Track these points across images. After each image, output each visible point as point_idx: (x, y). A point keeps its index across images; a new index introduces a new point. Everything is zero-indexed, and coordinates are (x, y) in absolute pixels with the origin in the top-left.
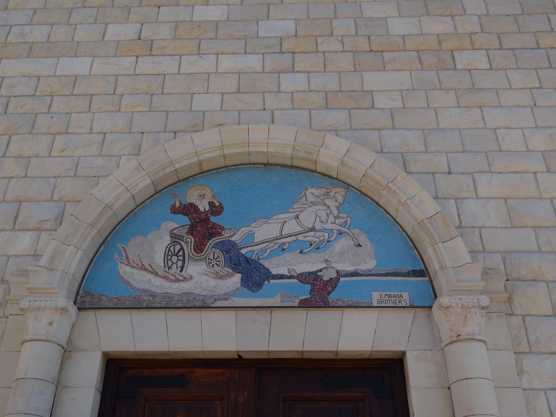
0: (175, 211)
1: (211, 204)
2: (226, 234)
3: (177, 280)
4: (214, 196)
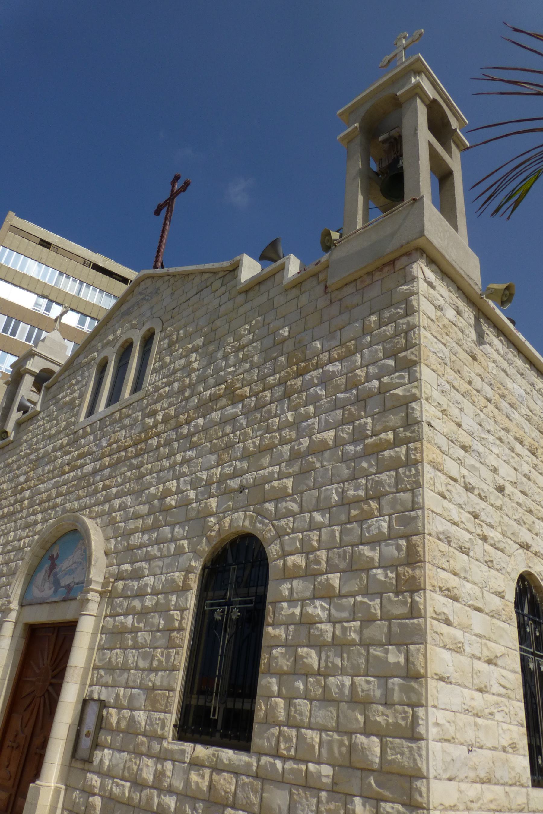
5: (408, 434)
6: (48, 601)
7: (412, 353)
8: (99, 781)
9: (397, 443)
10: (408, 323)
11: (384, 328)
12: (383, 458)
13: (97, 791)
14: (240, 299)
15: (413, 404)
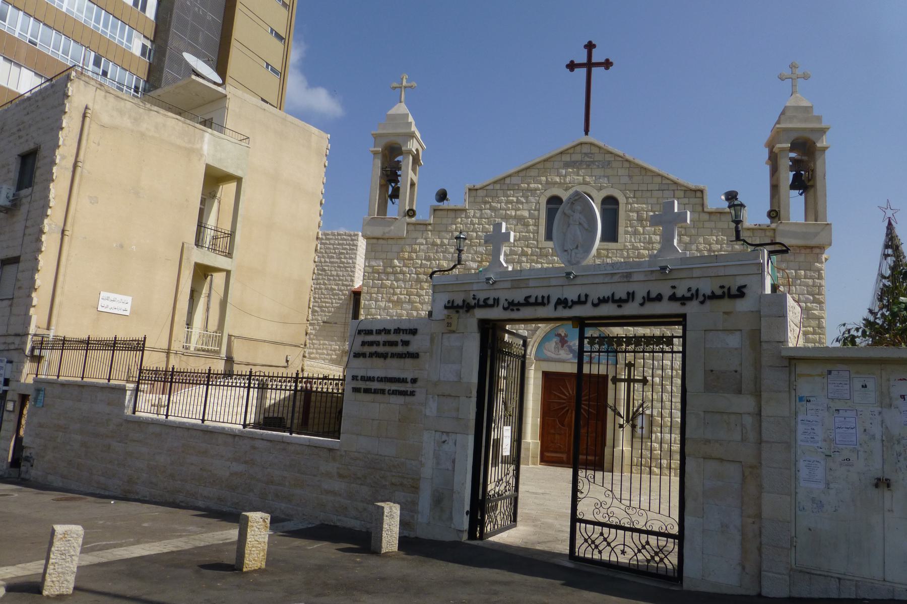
0: (556, 335)
1: (565, 334)
2: (569, 343)
3: (557, 355)
9: (814, 333)
10: (820, 283)
12: (809, 338)
13: (658, 449)
14: (706, 217)
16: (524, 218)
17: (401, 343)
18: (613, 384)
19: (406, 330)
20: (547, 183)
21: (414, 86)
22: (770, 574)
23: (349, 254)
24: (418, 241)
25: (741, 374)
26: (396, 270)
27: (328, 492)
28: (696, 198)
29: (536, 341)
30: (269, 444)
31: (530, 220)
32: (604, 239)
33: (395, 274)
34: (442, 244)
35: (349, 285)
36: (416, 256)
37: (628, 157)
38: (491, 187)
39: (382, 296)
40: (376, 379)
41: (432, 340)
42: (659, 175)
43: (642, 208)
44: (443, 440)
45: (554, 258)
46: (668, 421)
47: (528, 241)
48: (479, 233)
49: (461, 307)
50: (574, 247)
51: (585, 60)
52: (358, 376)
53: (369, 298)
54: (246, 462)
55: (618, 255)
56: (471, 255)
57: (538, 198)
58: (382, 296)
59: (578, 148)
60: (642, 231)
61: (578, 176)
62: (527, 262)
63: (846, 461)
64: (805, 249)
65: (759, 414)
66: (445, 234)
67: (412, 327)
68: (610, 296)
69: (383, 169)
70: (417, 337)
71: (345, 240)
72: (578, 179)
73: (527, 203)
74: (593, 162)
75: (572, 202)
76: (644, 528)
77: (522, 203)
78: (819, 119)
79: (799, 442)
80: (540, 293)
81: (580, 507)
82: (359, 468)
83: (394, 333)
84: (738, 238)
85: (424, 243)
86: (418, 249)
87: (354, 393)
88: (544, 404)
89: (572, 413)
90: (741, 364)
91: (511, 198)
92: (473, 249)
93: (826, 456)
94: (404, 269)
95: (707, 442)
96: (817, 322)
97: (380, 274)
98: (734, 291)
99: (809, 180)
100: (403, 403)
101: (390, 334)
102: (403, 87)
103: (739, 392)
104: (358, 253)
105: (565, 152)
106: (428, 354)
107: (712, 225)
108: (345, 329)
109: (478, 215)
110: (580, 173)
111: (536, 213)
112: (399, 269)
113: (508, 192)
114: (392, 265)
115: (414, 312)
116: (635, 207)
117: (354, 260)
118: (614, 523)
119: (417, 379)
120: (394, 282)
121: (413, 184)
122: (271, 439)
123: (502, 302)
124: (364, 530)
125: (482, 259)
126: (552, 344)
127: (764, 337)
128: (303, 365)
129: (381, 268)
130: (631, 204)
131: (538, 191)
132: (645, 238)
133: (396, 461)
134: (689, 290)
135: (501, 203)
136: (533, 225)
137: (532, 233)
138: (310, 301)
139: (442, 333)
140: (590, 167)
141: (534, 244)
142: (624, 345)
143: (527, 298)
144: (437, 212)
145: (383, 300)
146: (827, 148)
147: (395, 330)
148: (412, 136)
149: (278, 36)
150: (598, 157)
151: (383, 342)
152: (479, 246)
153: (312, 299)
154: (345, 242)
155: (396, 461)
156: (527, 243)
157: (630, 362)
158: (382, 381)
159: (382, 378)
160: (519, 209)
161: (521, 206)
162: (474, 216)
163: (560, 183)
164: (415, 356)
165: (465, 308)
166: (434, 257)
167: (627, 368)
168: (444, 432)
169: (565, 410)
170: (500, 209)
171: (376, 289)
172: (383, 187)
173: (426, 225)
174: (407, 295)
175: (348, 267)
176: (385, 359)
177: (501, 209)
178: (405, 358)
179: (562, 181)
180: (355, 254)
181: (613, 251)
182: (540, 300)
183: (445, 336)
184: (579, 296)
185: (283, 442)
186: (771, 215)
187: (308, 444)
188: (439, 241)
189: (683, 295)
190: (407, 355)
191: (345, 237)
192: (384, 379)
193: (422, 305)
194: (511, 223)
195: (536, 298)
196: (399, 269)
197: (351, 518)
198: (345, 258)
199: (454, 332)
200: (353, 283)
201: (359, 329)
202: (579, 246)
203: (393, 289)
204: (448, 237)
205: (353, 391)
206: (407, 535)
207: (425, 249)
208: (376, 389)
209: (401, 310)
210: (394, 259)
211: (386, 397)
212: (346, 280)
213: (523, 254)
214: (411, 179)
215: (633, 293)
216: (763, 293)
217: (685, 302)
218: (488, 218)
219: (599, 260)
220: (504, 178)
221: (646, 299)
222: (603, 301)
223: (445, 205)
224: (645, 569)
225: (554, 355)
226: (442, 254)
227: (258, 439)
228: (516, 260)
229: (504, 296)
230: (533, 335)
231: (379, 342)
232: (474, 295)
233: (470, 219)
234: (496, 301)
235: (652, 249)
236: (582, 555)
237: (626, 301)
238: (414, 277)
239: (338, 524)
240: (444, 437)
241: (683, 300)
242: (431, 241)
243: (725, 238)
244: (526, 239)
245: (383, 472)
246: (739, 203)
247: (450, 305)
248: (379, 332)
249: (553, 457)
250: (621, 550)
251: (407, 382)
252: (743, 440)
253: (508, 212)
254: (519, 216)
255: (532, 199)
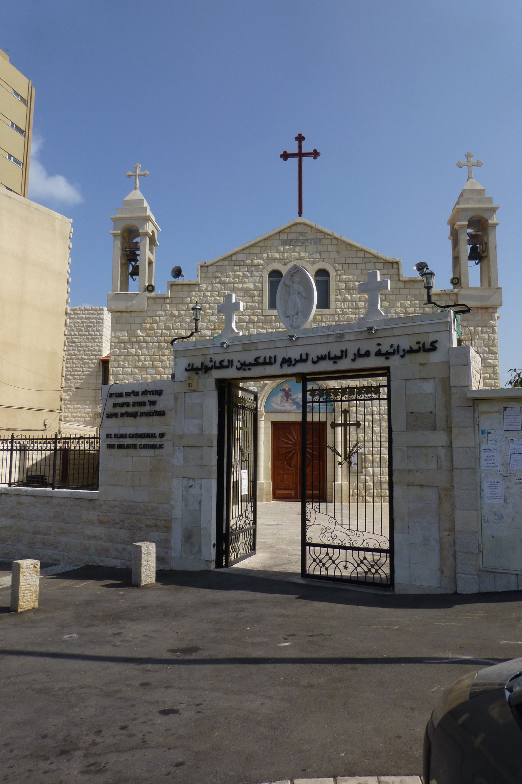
0: (281, 390)
1: (289, 389)
2: (292, 396)
3: (283, 407)
4: (289, 387)
5: (495, 377)
6: (292, 412)
7: (496, 349)
8: (369, 478)
9: (490, 378)
10: (494, 337)
11: (484, 335)
12: (486, 382)
13: (369, 481)
14: (401, 285)
15: (496, 367)
16: (250, 290)
17: (149, 403)
18: (332, 428)
19: (153, 391)
20: (268, 258)
21: (147, 174)
22: (463, 576)
23: (96, 327)
24: (158, 313)
25: (435, 415)
26: (140, 339)
27: (90, 537)
28: (393, 269)
29: (264, 396)
30: (33, 499)
31: (255, 292)
32: (319, 306)
33: (139, 343)
34: (180, 315)
35: (98, 355)
36: (157, 326)
37: (336, 235)
38: (219, 264)
39: (129, 363)
40: (128, 436)
41: (176, 399)
42: (362, 250)
43: (349, 279)
44: (190, 485)
45: (277, 323)
46: (376, 457)
47: (254, 310)
48: (212, 304)
49: (200, 369)
50: (295, 314)
51: (296, 151)
52: (111, 434)
53: (116, 365)
54: (13, 517)
55: (331, 319)
56: (205, 324)
57: (261, 272)
58: (129, 363)
59: (294, 228)
60: (349, 299)
61: (294, 252)
62: (254, 329)
63: (519, 480)
64: (482, 309)
65: (451, 447)
66: (182, 306)
67: (157, 389)
68: (327, 354)
69: (123, 249)
70: (162, 397)
71: (92, 314)
72: (294, 255)
73: (251, 276)
74: (307, 240)
75: (292, 275)
76: (362, 546)
77: (247, 277)
78: (490, 200)
79: (483, 468)
80: (268, 354)
81: (309, 534)
82: (117, 514)
83: (142, 395)
84: (429, 301)
85: (164, 314)
86: (158, 321)
87: (109, 449)
88: (273, 449)
89: (297, 456)
90: (435, 406)
91: (238, 273)
92: (207, 319)
93: (504, 477)
94: (147, 338)
95: (410, 471)
96: (493, 370)
97: (126, 344)
98: (428, 346)
99: (483, 252)
100: (153, 456)
101: (138, 395)
102: (137, 176)
103: (434, 429)
104: (104, 325)
105: (284, 231)
106: (173, 411)
107: (406, 291)
108: (96, 394)
109: (210, 289)
110: (296, 249)
111: (260, 285)
112: (142, 339)
113: (235, 268)
114: (136, 335)
115: (157, 375)
116: (343, 278)
117: (101, 332)
118: (337, 544)
119: (164, 433)
120: (139, 350)
121: (150, 263)
122: (35, 495)
123: (236, 363)
124: (124, 568)
125: (215, 327)
126: (278, 398)
127: (453, 383)
128: (60, 427)
129: (126, 338)
130: (340, 276)
131: (260, 266)
132: (352, 304)
133: (150, 506)
134: (392, 346)
135: (229, 278)
136: (257, 296)
137: (257, 303)
138: (62, 370)
139: (185, 393)
140: (305, 244)
141: (258, 312)
142: (340, 395)
143: (256, 359)
144: (174, 287)
145: (129, 366)
146: (497, 224)
147: (142, 392)
148: (147, 219)
149: (18, 129)
150: (311, 236)
151: (133, 403)
152: (212, 316)
153: (65, 369)
154: (92, 316)
155: (150, 506)
156: (253, 311)
157: (345, 409)
158: (134, 438)
159: (133, 434)
160: (245, 283)
161: (246, 280)
162: (206, 290)
163: (280, 259)
164: (161, 414)
165: (203, 369)
166: (173, 326)
167: (343, 415)
168: (191, 478)
169: (292, 453)
170: (229, 283)
171: (123, 357)
172: (124, 266)
173: (164, 298)
174: (150, 361)
175: (95, 339)
176: (135, 418)
177: (229, 283)
178: (152, 416)
179: (281, 257)
180: (102, 326)
181: (326, 316)
182: (268, 360)
183: (187, 394)
184: (301, 355)
185: (47, 497)
186: (454, 282)
187: (70, 496)
188: (176, 313)
189: (387, 351)
190: (155, 414)
191: (91, 312)
192: (135, 436)
193: (164, 370)
194: (239, 294)
195: (265, 358)
196: (143, 338)
197: (112, 558)
198: (93, 330)
199: (194, 391)
200: (101, 353)
201: (109, 392)
202: (299, 311)
203: (138, 356)
204: (184, 308)
205: (108, 448)
206: (162, 568)
207: (165, 320)
208: (129, 444)
209: (146, 374)
210: (137, 330)
211: (138, 451)
212: (95, 350)
213: (251, 321)
214: (149, 257)
215: (346, 350)
216: (451, 346)
217: (389, 357)
218: (218, 291)
219: (315, 325)
220: (231, 256)
221: (357, 355)
222: (321, 358)
223: (180, 280)
224: (363, 580)
225: (280, 407)
226: (180, 324)
227: (23, 495)
228: (245, 327)
229: (237, 358)
230: (262, 391)
231: (129, 403)
232: (211, 358)
233: (203, 293)
234: (231, 363)
235: (359, 314)
236: (312, 573)
237: (340, 358)
238: (155, 345)
239: (101, 564)
240: (191, 483)
241: (387, 355)
242: (170, 312)
243: (418, 302)
244: (253, 308)
245: (138, 516)
246: (430, 272)
247: (190, 368)
248: (128, 394)
249: (283, 494)
250: (344, 566)
251: (156, 437)
252: (439, 468)
253: (236, 285)
254: (245, 288)
255: (256, 273)
